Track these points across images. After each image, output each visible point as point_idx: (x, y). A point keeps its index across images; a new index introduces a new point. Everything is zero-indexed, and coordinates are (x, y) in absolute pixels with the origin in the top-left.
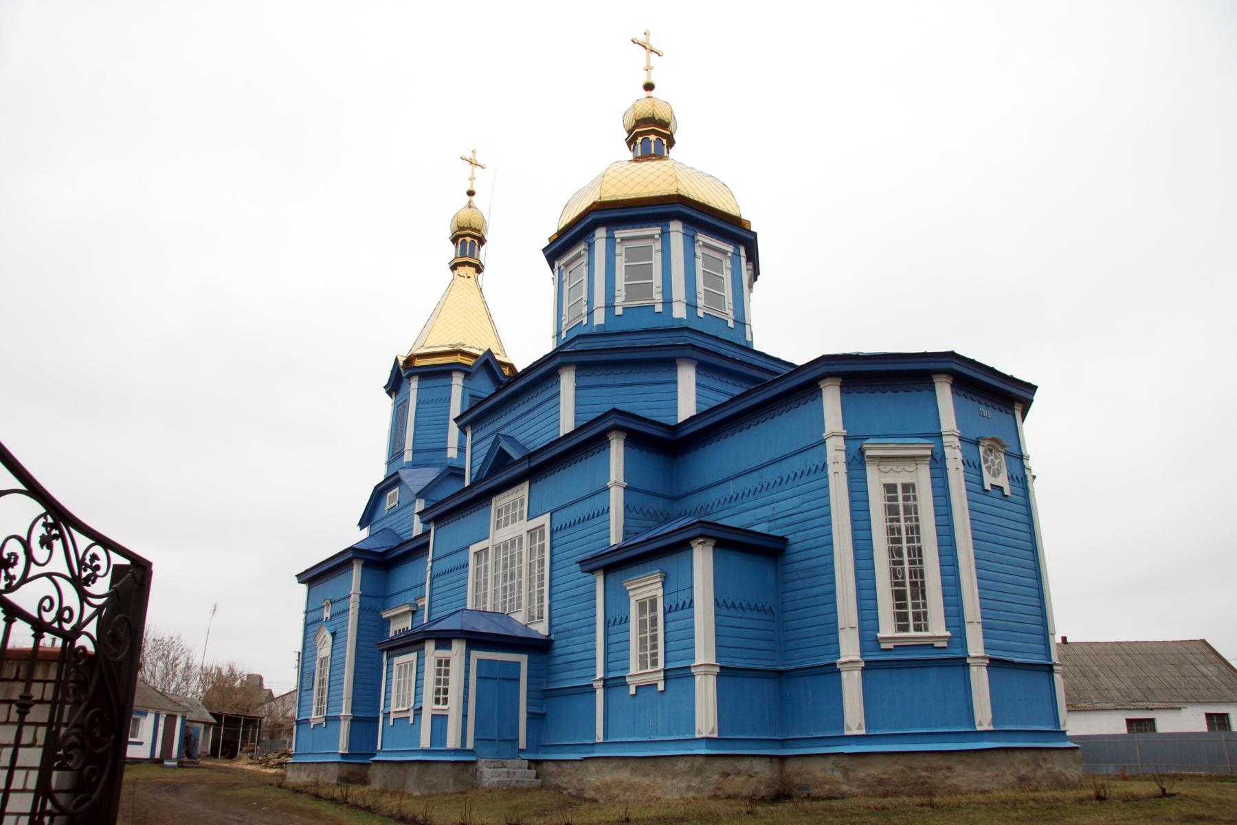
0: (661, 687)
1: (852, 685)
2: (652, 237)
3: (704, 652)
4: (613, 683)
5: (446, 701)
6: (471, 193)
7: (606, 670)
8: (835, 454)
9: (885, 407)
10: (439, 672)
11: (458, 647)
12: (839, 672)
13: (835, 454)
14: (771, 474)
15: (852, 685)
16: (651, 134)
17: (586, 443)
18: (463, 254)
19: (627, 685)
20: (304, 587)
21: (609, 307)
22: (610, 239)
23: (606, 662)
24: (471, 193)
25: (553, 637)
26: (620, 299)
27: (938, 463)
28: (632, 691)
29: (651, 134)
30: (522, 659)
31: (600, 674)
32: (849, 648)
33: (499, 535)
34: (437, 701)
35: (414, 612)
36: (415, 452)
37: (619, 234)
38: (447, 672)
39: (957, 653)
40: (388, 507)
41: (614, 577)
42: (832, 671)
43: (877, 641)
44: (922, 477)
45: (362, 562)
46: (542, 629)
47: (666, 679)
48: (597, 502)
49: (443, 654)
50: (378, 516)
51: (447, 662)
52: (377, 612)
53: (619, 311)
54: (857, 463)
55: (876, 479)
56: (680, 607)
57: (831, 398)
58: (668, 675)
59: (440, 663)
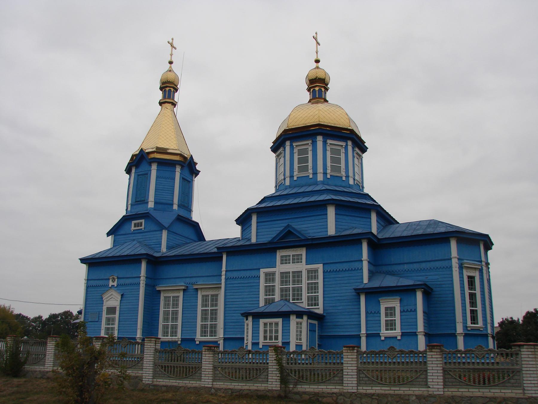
0: (399, 338)
1: (460, 341)
2: (342, 146)
3: (421, 328)
4: (372, 336)
5: (300, 339)
6: (171, 63)
7: (367, 330)
8: (455, 263)
10: (297, 328)
11: (305, 318)
12: (456, 336)
13: (455, 263)
14: (423, 265)
15: (460, 341)
16: (318, 86)
18: (164, 97)
19: (380, 336)
20: (84, 267)
21: (325, 173)
22: (325, 143)
23: (367, 327)
24: (171, 63)
25: (325, 314)
26: (329, 171)
29: (318, 86)
31: (363, 331)
32: (460, 329)
33: (280, 268)
34: (297, 339)
35: (184, 290)
36: (156, 203)
37: (329, 141)
38: (301, 328)
39: (484, 332)
40: (133, 228)
42: (454, 336)
43: (467, 327)
44: (477, 275)
45: (147, 260)
47: (402, 336)
49: (299, 320)
50: (122, 232)
51: (301, 324)
52: (154, 286)
53: (329, 176)
54: (461, 267)
55: (466, 273)
56: (408, 312)
57: (453, 244)
58: (403, 334)
59: (297, 323)
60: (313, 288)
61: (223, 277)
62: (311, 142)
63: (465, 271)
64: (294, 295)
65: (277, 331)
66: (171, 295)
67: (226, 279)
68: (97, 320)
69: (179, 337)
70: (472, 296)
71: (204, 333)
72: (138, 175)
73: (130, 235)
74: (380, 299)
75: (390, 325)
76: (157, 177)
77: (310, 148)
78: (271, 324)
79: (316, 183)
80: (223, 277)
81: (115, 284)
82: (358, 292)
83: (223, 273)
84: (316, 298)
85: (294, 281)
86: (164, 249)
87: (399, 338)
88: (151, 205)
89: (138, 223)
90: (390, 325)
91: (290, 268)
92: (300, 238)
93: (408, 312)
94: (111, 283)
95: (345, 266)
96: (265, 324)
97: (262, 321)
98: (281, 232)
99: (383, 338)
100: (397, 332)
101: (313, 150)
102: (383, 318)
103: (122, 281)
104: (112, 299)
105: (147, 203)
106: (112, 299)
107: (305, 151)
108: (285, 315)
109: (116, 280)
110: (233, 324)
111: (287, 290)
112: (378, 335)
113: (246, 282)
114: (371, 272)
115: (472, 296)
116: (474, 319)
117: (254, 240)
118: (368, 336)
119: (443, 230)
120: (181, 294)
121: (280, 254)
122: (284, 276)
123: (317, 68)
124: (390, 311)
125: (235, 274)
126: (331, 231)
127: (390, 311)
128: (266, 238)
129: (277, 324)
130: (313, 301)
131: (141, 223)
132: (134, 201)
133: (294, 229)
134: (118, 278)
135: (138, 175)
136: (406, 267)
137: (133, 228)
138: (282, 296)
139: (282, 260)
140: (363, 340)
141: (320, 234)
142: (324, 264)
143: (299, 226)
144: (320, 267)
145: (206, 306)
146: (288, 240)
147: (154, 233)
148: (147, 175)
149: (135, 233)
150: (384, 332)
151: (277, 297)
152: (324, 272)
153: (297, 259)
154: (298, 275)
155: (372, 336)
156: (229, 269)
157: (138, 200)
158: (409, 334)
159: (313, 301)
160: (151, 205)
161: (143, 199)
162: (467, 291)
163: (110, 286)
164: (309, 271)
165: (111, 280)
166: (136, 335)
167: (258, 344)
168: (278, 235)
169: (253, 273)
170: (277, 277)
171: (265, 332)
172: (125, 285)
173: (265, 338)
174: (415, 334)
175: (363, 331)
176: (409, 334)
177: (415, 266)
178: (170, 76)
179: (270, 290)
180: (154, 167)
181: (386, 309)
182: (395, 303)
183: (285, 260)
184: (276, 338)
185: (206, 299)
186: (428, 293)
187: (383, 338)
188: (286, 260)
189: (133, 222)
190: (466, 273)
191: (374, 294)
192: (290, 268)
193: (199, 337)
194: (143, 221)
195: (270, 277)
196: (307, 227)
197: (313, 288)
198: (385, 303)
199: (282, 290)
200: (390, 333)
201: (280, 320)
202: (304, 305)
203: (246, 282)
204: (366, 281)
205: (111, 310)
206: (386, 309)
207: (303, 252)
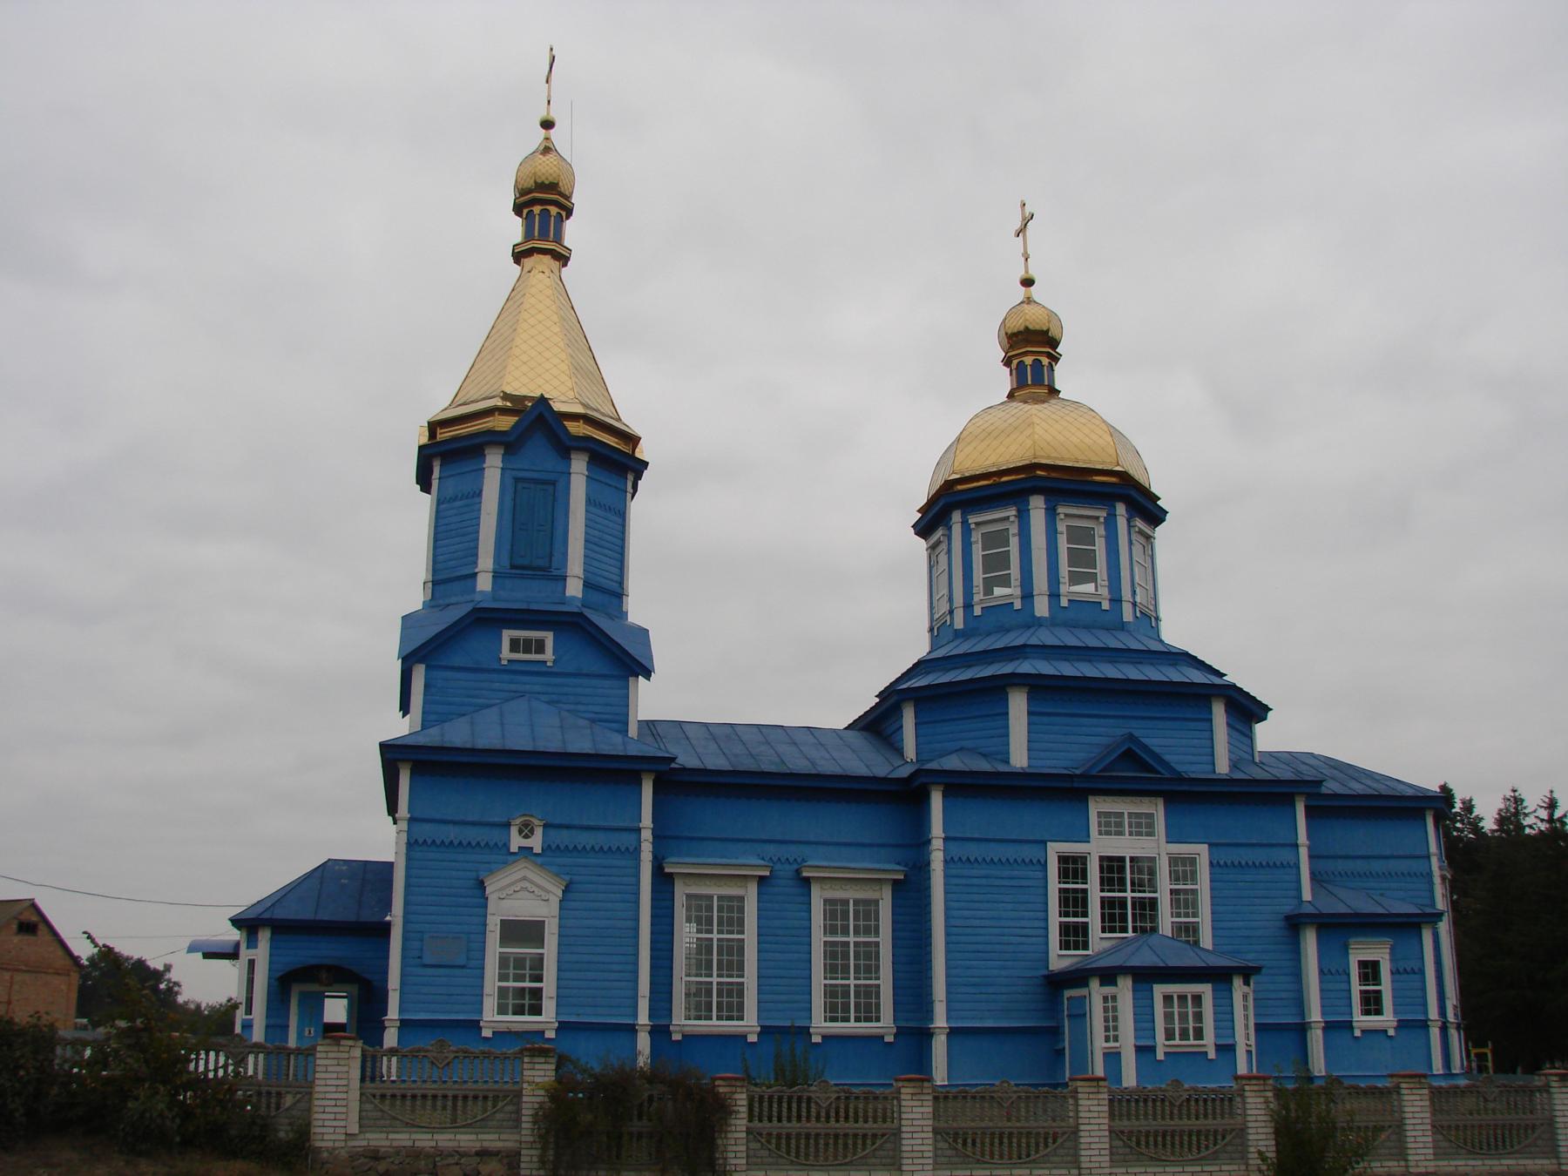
4: (1337, 1027)
6: (547, 125)
16: (1031, 351)
24: (547, 125)
28: (1357, 1033)
29: (1031, 351)
36: (588, 585)
56: (1408, 972)
58: (1402, 1025)
62: (1103, 514)
65: (1198, 1017)
66: (715, 890)
68: (461, 961)
69: (749, 1023)
71: (835, 1010)
72: (517, 480)
73: (495, 676)
74: (1352, 940)
75: (1372, 1003)
76: (590, 501)
77: (1100, 531)
78: (1182, 998)
79: (1122, 626)
81: (536, 842)
82: (1294, 924)
88: (574, 588)
92: (1158, 772)
93: (1408, 972)
94: (516, 841)
95: (1260, 855)
96: (1168, 999)
97: (1159, 990)
100: (1387, 1019)
101: (1107, 538)
102: (1356, 988)
103: (564, 838)
104: (523, 894)
105: (564, 578)
106: (523, 894)
107: (1088, 536)
108: (1219, 977)
109: (539, 832)
110: (972, 990)
112: (1349, 1026)
113: (1007, 873)
114: (1314, 877)
118: (1329, 1027)
119: (1410, 792)
120: (751, 893)
121: (1097, 807)
122: (1113, 868)
123: (1029, 300)
124: (1370, 971)
125: (973, 851)
127: (1370, 971)
128: (1056, 763)
129: (1197, 999)
132: (506, 562)
133: (1145, 748)
134: (545, 826)
135: (517, 480)
136: (1341, 865)
137: (506, 653)
140: (1316, 1038)
141: (1193, 768)
142: (1210, 845)
144: (1201, 851)
146: (1133, 773)
147: (595, 682)
148: (555, 488)
149: (514, 669)
150: (1361, 1020)
152: (1211, 864)
153: (1143, 826)
155: (1337, 1027)
156: (952, 834)
157: (520, 562)
158: (1413, 1026)
160: (574, 588)
161: (541, 563)
163: (514, 849)
164: (1174, 860)
165: (514, 831)
166: (636, 1016)
167: (1152, 1049)
169: (1028, 852)
171: (1168, 1017)
172: (575, 850)
173: (1169, 1035)
177: (1360, 866)
178: (546, 168)
180: (579, 465)
181: (1363, 964)
183: (1112, 825)
184: (1199, 1034)
187: (1357, 1033)
189: (507, 635)
191: (1338, 928)
192: (1125, 846)
193: (820, 1024)
194: (549, 637)
195: (1073, 868)
196: (1167, 741)
198: (1361, 951)
200: (1372, 1021)
201: (1206, 990)
203: (1007, 873)
204: (1307, 895)
205: (523, 932)
206: (1363, 964)
207: (1157, 810)
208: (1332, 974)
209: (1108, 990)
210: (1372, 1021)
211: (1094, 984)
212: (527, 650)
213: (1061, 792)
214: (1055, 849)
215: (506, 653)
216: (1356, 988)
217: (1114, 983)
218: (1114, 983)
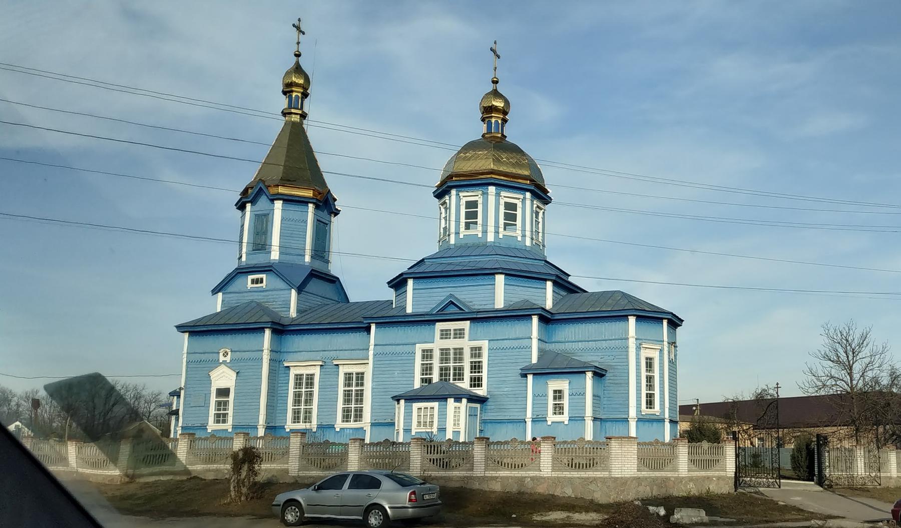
0: (566, 423)
1: (633, 425)
3: (589, 412)
4: (538, 420)
7: (533, 414)
8: (632, 343)
9: (650, 329)
13: (632, 343)
15: (633, 425)
17: (516, 315)
27: (661, 351)
30: (478, 406)
31: (529, 414)
32: (633, 413)
41: (542, 379)
42: (626, 420)
44: (655, 355)
46: (481, 392)
48: (525, 342)
54: (638, 348)
57: (632, 320)
58: (571, 419)
60: (476, 367)
61: (371, 353)
63: (642, 351)
64: (455, 375)
67: (375, 355)
70: (650, 379)
75: (558, 409)
80: (371, 353)
83: (372, 347)
84: (479, 379)
85: (455, 359)
86: (293, 313)
87: (566, 423)
89: (257, 280)
90: (558, 409)
91: (452, 343)
98: (443, 301)
99: (549, 423)
100: (565, 418)
105: (270, 252)
111: (447, 369)
115: (650, 379)
116: (650, 403)
117: (409, 310)
118: (534, 421)
121: (440, 326)
122: (444, 352)
124: (558, 394)
126: (500, 304)
127: (558, 394)
128: (422, 310)
130: (476, 382)
131: (262, 279)
133: (457, 299)
137: (250, 285)
138: (441, 375)
139: (442, 335)
143: (463, 296)
144: (485, 344)
145: (349, 385)
150: (551, 418)
151: (436, 378)
153: (459, 334)
154: (459, 352)
155: (538, 420)
158: (577, 419)
159: (476, 382)
160: (275, 255)
162: (644, 374)
168: (436, 307)
169: (407, 349)
170: (437, 355)
174: (583, 419)
175: (529, 414)
176: (577, 419)
179: (427, 369)
181: (555, 391)
182: (562, 384)
183: (445, 334)
185: (349, 378)
186: (599, 374)
187: (549, 423)
188: (447, 334)
190: (644, 354)
192: (452, 343)
194: (264, 276)
195: (427, 354)
197: (476, 367)
198: (554, 384)
199: (441, 369)
200: (558, 418)
202: (465, 384)
207: (466, 325)
208: (540, 397)
209: (457, 404)
210: (558, 418)
211: (451, 401)
212: (257, 283)
213: (425, 321)
214: (419, 348)
215: (250, 285)
216: (551, 402)
217: (461, 402)
218: (461, 402)
